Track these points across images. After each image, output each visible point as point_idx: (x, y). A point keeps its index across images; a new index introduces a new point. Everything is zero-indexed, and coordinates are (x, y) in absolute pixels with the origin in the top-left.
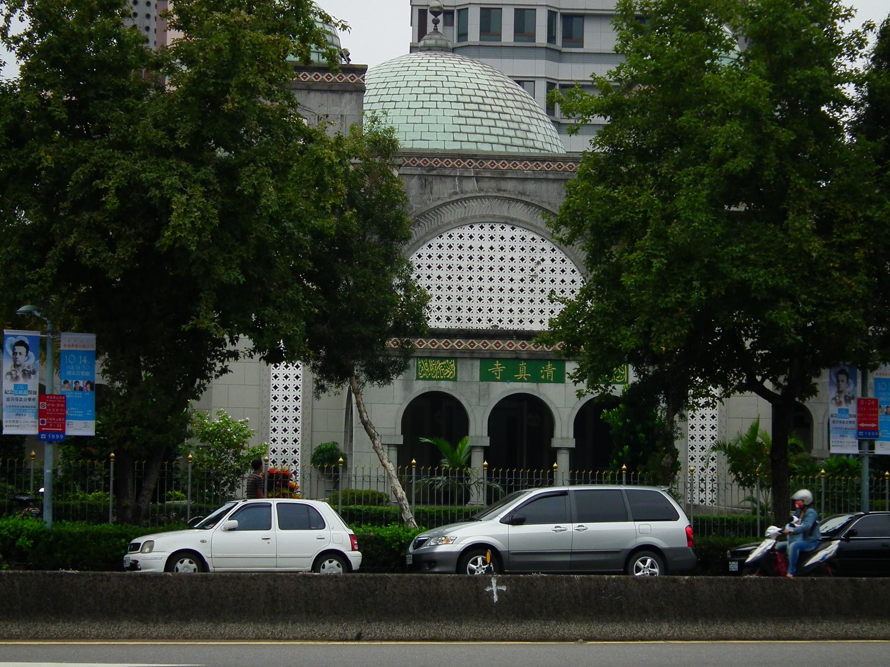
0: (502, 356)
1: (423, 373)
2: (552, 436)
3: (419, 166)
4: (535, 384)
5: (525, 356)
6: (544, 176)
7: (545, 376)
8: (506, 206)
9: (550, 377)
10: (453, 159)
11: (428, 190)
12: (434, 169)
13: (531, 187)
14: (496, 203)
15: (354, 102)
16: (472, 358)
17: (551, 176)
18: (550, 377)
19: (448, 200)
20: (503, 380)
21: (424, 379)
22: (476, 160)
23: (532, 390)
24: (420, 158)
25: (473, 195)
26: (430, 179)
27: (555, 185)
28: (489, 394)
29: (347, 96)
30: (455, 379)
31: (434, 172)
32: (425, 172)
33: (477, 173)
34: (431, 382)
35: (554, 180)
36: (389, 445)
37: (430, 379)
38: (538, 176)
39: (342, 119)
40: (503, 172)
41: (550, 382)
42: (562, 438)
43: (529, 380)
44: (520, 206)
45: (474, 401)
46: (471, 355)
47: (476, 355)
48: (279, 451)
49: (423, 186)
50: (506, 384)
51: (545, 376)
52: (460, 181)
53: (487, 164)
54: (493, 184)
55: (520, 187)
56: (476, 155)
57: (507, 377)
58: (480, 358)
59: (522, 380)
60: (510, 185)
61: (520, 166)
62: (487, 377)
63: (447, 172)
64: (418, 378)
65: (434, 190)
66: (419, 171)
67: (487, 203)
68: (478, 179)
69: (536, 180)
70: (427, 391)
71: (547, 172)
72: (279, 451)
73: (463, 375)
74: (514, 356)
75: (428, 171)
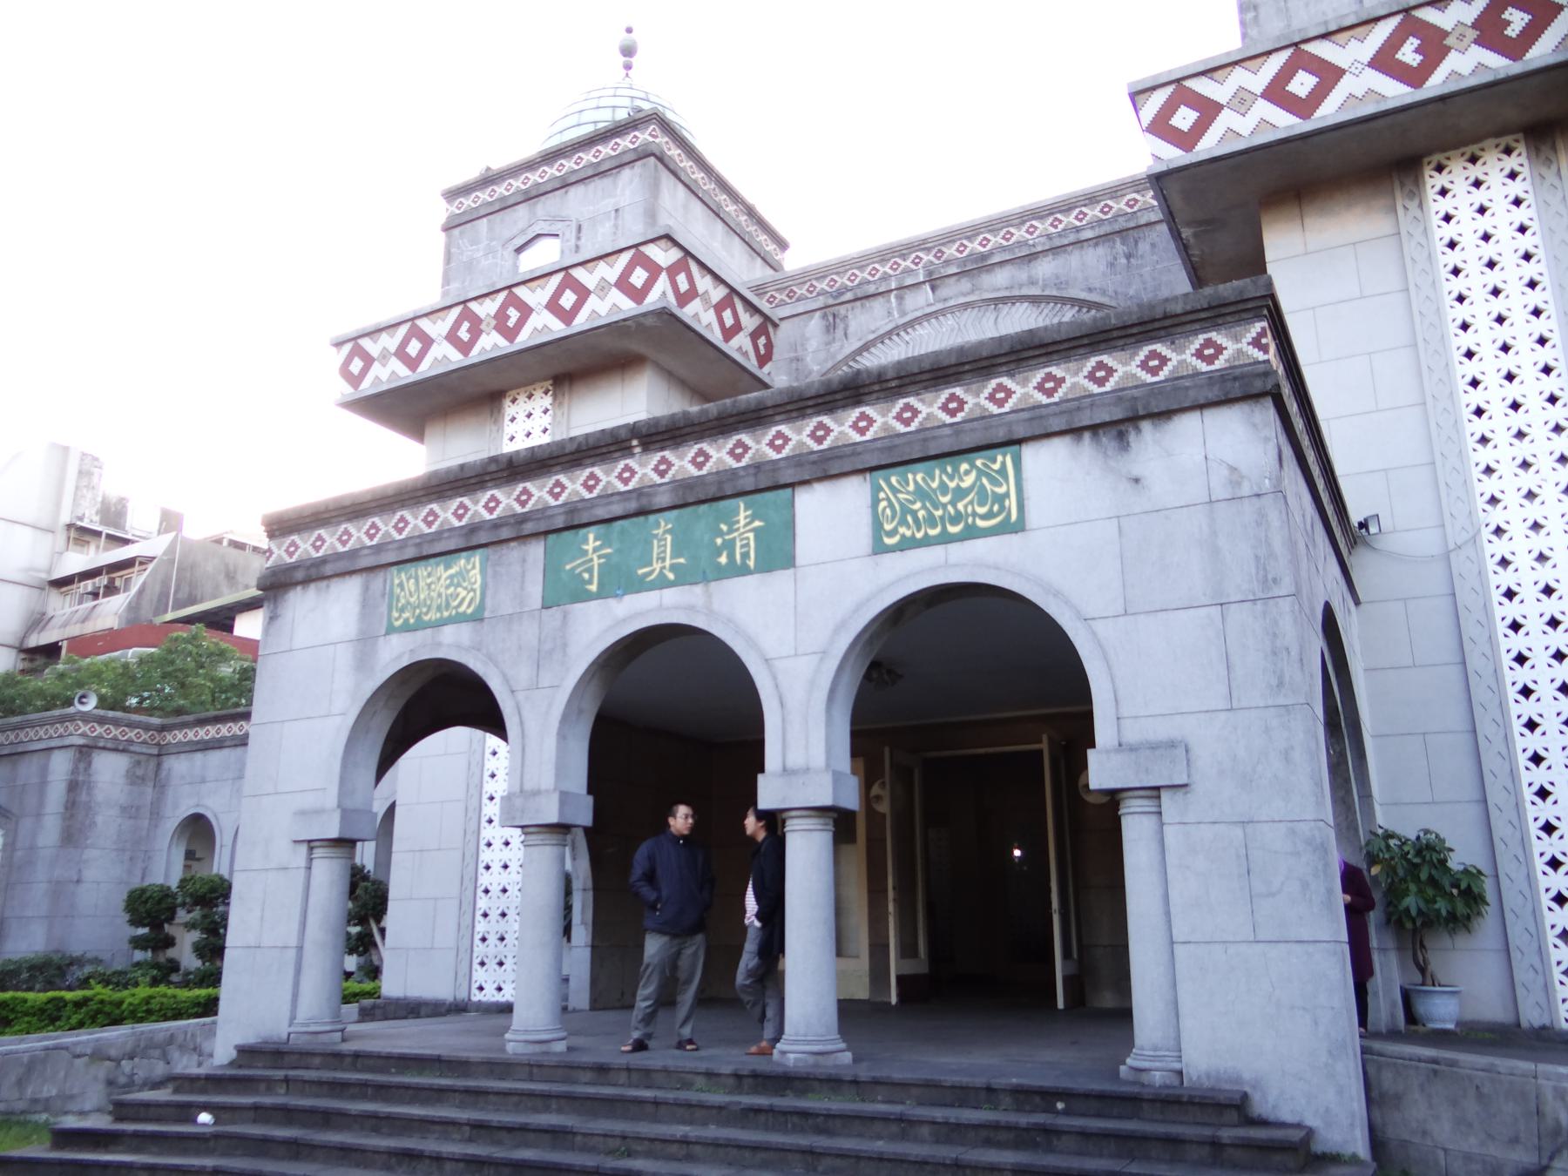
0: (601, 513)
1: (402, 610)
2: (756, 763)
3: (822, 293)
4: (698, 589)
5: (663, 499)
6: (1072, 238)
7: (731, 556)
8: (990, 315)
9: (745, 556)
10: (883, 261)
11: (839, 332)
12: (848, 290)
13: (1045, 268)
14: (969, 315)
15: (636, 180)
16: (522, 538)
17: (1088, 234)
18: (745, 556)
19: (871, 337)
20: (601, 595)
21: (407, 628)
22: (929, 250)
23: (691, 608)
24: (820, 278)
25: (919, 314)
26: (842, 310)
27: (1101, 250)
28: (565, 646)
29: (626, 173)
30: (477, 618)
31: (849, 296)
32: (831, 301)
33: (930, 273)
34: (420, 633)
35: (1097, 240)
36: (311, 844)
37: (420, 625)
38: (1057, 242)
39: (616, 218)
40: (984, 257)
41: (744, 571)
42: (786, 771)
43: (684, 577)
44: (1022, 308)
45: (523, 674)
46: (519, 530)
47: (529, 527)
48: (495, 890)
49: (830, 328)
50: (612, 602)
51: (731, 556)
52: (900, 299)
53: (951, 251)
54: (965, 284)
55: (1021, 274)
56: (925, 241)
57: (619, 581)
58: (547, 533)
59: (662, 583)
60: (1000, 280)
61: (1019, 234)
62: (564, 592)
63: (872, 289)
64: (391, 630)
65: (851, 330)
66: (821, 302)
67: (949, 321)
68: (934, 282)
69: (1055, 250)
70: (405, 662)
71: (1078, 230)
72: (495, 890)
73: (503, 602)
74: (633, 506)
75: (835, 298)
